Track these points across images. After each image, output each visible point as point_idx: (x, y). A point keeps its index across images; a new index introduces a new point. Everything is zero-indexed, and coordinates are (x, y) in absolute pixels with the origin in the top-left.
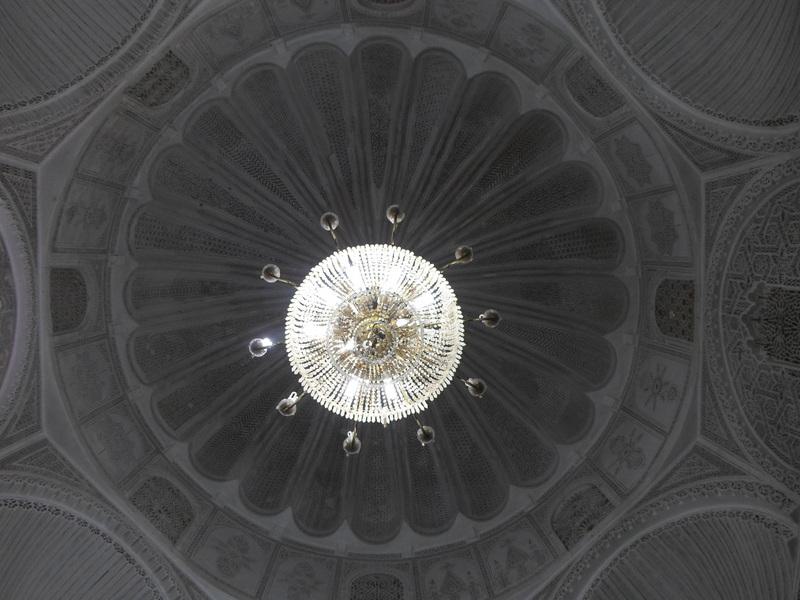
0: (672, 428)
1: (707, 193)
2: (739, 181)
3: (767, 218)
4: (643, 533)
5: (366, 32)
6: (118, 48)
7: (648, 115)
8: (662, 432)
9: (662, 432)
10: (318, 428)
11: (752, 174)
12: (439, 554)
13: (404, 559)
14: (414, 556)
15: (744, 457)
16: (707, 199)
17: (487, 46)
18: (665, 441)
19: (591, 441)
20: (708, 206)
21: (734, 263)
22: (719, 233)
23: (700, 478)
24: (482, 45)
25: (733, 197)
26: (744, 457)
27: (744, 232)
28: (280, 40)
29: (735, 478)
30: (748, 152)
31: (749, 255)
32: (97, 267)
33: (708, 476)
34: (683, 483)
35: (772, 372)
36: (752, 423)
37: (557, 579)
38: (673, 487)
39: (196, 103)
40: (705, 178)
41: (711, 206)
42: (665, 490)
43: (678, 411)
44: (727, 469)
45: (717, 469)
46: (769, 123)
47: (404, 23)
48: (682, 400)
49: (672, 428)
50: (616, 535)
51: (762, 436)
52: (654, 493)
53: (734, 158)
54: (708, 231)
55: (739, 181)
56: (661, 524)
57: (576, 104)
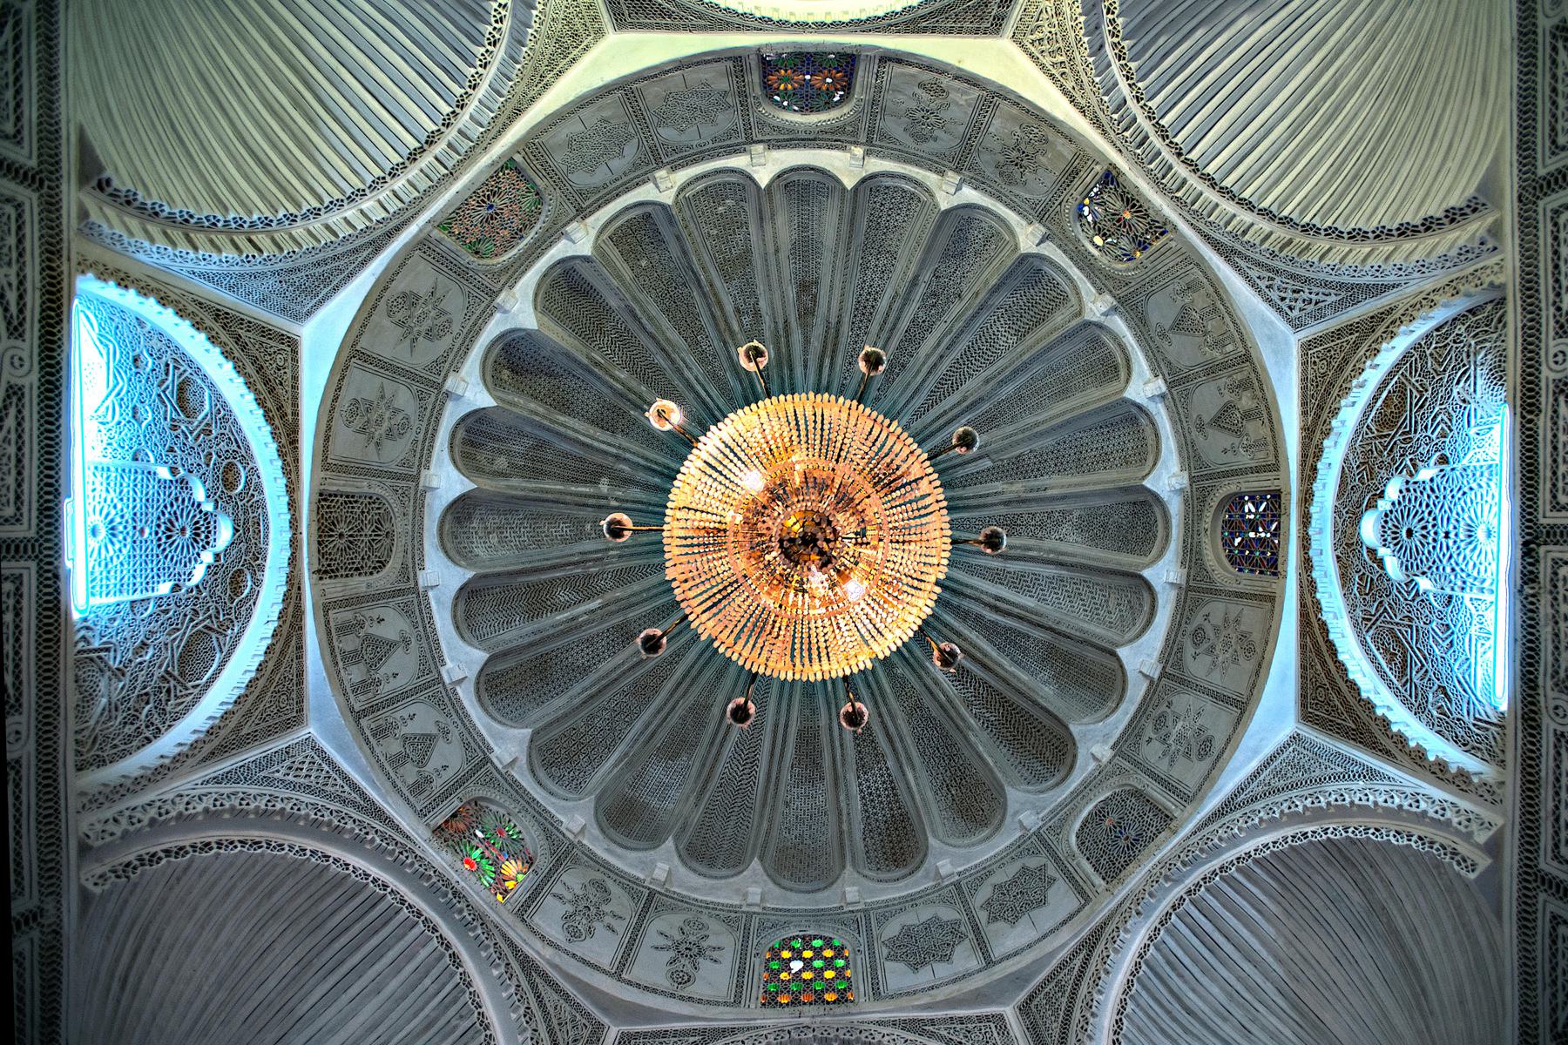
0: (630, 983)
1: (988, 1018)
5: (1175, 507)
6: (1179, 155)
7: (1099, 919)
8: (622, 965)
9: (622, 965)
10: (609, 444)
12: (424, 627)
13: (415, 574)
14: (421, 590)
16: (979, 1019)
17: (1164, 674)
18: (604, 972)
19: (599, 847)
20: (969, 1018)
24: (1164, 668)
28: (1164, 389)
32: (849, 128)
34: (546, 1013)
37: (388, 821)
38: (538, 997)
39: (1075, 273)
40: (1009, 1012)
41: (970, 1026)
43: (655, 991)
47: (1192, 556)
48: (672, 995)
49: (630, 983)
50: (460, 911)
54: (932, 1022)
56: (479, 985)
57: (1090, 807)
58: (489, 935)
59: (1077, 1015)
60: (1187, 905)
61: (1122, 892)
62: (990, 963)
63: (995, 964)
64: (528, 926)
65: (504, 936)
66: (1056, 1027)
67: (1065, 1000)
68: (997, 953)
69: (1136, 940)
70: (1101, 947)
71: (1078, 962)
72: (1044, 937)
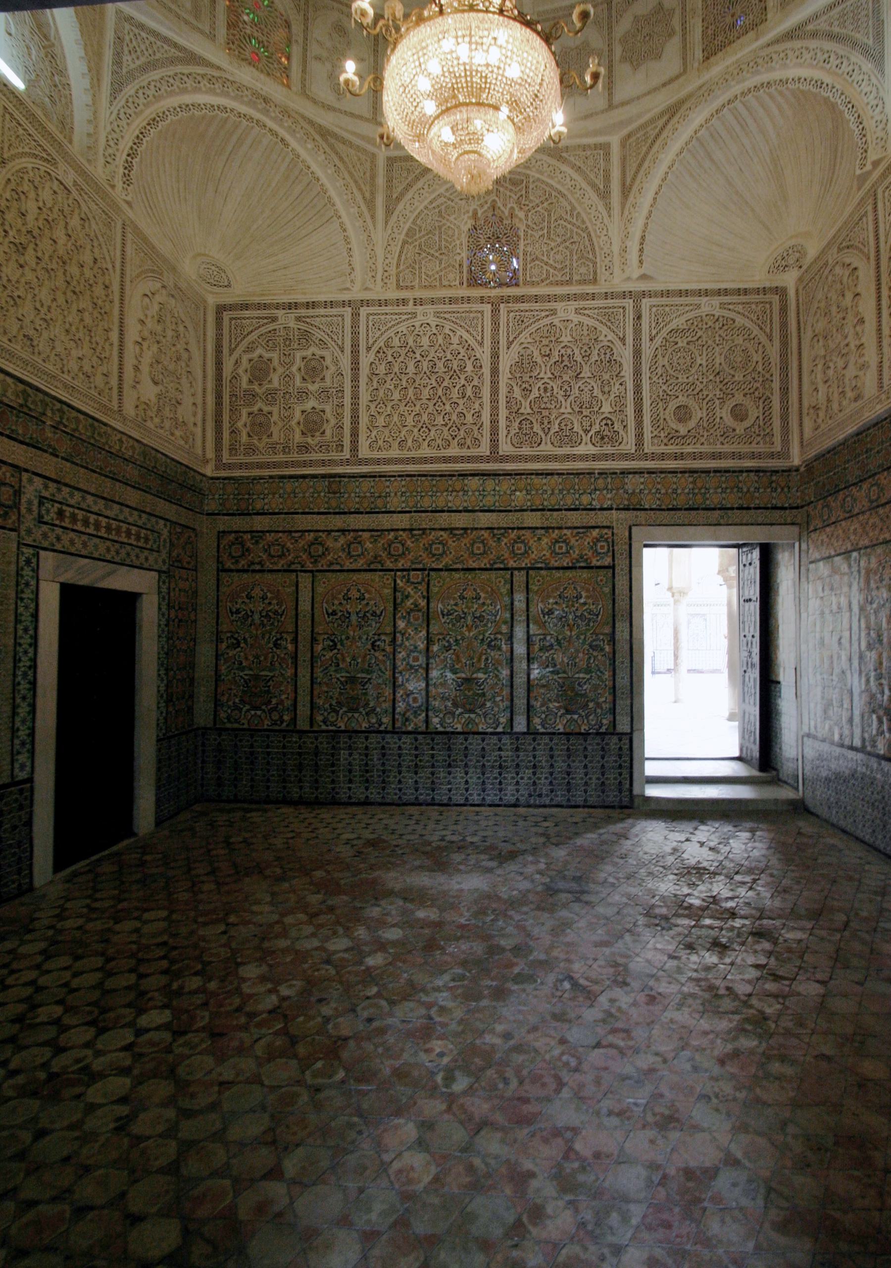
2: (604, 195)
3: (574, 225)
4: (288, 137)
11: (609, 209)
15: (386, 223)
18: (367, 120)
21: (539, 184)
22: (565, 168)
23: (356, 182)
25: (594, 186)
26: (386, 223)
27: (564, 196)
29: (369, 220)
30: (626, 212)
31: (545, 205)
33: (360, 189)
35: (458, 242)
36: (414, 223)
40: (615, 141)
42: (332, 147)
44: (371, 204)
45: (367, 195)
46: (643, 238)
51: (407, 235)
52: (324, 133)
53: (626, 191)
55: (604, 195)
58: (296, 122)
59: (646, 164)
60: (737, 104)
61: (706, 77)
62: (611, 106)
63: (617, 107)
64: (315, 102)
65: (303, 117)
66: (635, 165)
67: (644, 149)
68: (618, 97)
69: (698, 118)
70: (675, 119)
71: (660, 123)
72: (649, 93)
